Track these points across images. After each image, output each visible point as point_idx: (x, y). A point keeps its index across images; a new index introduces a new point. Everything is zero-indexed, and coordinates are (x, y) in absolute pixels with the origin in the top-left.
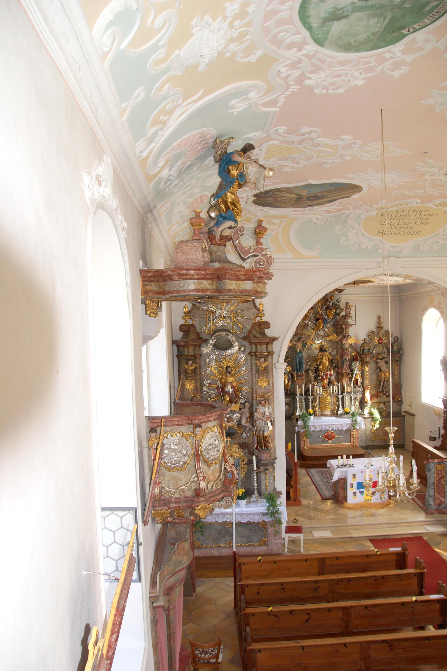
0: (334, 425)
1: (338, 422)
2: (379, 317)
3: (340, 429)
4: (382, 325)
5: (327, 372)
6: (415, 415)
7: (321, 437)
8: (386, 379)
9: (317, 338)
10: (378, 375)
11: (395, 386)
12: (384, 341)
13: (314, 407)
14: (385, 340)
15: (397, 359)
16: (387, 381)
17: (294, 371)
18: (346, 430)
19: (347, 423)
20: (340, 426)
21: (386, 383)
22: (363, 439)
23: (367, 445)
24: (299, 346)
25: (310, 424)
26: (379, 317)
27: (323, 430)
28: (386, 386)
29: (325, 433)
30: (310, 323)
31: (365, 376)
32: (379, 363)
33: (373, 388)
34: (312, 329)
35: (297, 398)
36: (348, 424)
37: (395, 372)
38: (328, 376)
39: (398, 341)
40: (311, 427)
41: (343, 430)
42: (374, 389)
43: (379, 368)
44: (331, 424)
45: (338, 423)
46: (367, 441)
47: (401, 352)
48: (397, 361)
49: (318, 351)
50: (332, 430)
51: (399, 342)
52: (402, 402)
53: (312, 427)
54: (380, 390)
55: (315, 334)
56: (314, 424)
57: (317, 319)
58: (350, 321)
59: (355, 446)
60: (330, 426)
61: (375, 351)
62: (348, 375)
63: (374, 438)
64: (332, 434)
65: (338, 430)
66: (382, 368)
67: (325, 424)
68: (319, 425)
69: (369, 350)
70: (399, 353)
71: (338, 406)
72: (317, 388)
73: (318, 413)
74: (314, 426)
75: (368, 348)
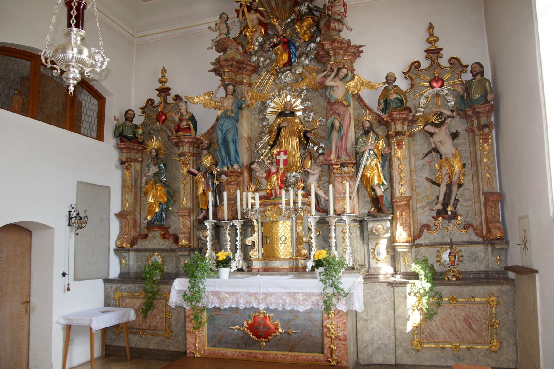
0: (271, 294)
1: (284, 287)
2: (431, 27)
3: (288, 308)
4: (438, 45)
5: (278, 157)
6: (536, 272)
7: (237, 327)
8: (455, 179)
9: (279, 92)
10: (433, 170)
11: (486, 199)
12: (446, 84)
13: (246, 249)
14: (449, 79)
15: (483, 121)
16: (460, 186)
17: (216, 166)
18: (306, 312)
19: (308, 291)
20: (288, 300)
21: (455, 188)
22: (386, 346)
23: (400, 362)
24: (226, 105)
25: (208, 289)
26: (431, 27)
27: (241, 307)
28: (457, 200)
29: (250, 317)
30: (262, 59)
31: (395, 174)
32: (432, 134)
33: (423, 207)
34: (268, 71)
35: (206, 224)
36: (313, 294)
37: (482, 161)
38: (281, 165)
39: (482, 73)
40: (210, 295)
41: (298, 312)
42: (427, 209)
43: (436, 150)
44: (263, 290)
45: (283, 291)
46: (400, 351)
47: (490, 97)
48: (486, 126)
49: (275, 116)
50: (267, 309)
51: (488, 75)
52: (507, 243)
53: (211, 298)
54: (439, 207)
55: (274, 80)
56: (218, 289)
57: (275, 45)
58: (345, 35)
59: (334, 363)
60: (261, 297)
61: (422, 110)
62: (343, 165)
63: (421, 343)
64: (268, 322)
65: (284, 311)
66: (442, 149)
67: (245, 290)
68: (234, 293)
69: (401, 101)
70: (487, 102)
71: (310, 245)
72: (254, 198)
73: (256, 265)
74: (217, 294)
75: (395, 96)
